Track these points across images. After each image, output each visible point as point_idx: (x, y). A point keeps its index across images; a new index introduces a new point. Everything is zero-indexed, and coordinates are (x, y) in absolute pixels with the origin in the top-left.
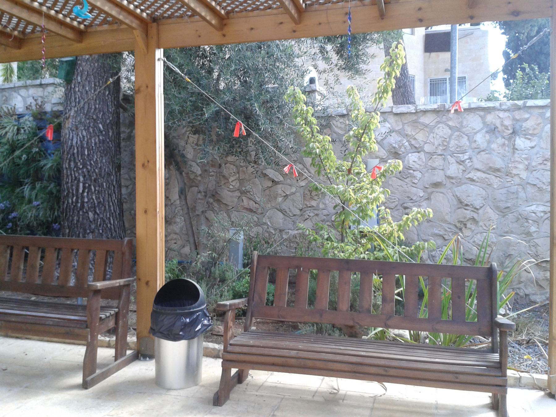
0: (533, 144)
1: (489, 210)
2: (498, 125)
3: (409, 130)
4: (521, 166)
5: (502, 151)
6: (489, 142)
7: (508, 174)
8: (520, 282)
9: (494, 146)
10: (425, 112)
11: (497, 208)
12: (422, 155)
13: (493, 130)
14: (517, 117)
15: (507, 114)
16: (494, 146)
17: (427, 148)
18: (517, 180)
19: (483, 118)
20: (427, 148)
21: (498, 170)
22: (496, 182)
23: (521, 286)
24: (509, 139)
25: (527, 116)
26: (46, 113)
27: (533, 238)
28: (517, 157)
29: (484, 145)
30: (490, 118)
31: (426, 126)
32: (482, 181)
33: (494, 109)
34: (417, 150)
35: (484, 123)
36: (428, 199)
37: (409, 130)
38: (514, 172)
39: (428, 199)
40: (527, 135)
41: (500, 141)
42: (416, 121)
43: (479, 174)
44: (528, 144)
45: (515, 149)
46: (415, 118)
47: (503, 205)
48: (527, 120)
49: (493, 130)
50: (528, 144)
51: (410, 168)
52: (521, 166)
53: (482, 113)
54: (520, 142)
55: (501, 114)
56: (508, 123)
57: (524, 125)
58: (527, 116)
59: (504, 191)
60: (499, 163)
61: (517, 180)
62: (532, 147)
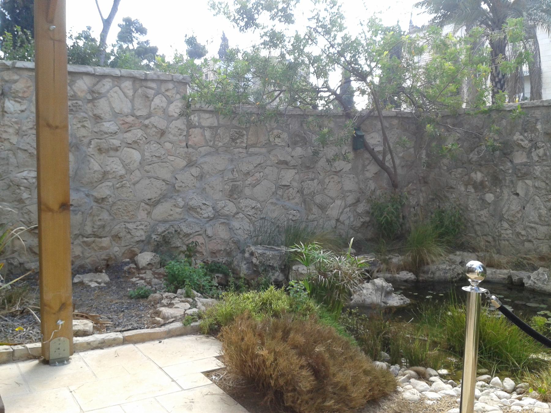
0: (23, 107)
4: (11, 130)
8: (14, 252)
14: (7, 78)
18: (7, 145)
23: (15, 255)
25: (16, 77)
27: (25, 205)
28: (6, 121)
48: (15, 82)
57: (14, 86)
58: (16, 77)
61: (7, 145)
62: (22, 111)
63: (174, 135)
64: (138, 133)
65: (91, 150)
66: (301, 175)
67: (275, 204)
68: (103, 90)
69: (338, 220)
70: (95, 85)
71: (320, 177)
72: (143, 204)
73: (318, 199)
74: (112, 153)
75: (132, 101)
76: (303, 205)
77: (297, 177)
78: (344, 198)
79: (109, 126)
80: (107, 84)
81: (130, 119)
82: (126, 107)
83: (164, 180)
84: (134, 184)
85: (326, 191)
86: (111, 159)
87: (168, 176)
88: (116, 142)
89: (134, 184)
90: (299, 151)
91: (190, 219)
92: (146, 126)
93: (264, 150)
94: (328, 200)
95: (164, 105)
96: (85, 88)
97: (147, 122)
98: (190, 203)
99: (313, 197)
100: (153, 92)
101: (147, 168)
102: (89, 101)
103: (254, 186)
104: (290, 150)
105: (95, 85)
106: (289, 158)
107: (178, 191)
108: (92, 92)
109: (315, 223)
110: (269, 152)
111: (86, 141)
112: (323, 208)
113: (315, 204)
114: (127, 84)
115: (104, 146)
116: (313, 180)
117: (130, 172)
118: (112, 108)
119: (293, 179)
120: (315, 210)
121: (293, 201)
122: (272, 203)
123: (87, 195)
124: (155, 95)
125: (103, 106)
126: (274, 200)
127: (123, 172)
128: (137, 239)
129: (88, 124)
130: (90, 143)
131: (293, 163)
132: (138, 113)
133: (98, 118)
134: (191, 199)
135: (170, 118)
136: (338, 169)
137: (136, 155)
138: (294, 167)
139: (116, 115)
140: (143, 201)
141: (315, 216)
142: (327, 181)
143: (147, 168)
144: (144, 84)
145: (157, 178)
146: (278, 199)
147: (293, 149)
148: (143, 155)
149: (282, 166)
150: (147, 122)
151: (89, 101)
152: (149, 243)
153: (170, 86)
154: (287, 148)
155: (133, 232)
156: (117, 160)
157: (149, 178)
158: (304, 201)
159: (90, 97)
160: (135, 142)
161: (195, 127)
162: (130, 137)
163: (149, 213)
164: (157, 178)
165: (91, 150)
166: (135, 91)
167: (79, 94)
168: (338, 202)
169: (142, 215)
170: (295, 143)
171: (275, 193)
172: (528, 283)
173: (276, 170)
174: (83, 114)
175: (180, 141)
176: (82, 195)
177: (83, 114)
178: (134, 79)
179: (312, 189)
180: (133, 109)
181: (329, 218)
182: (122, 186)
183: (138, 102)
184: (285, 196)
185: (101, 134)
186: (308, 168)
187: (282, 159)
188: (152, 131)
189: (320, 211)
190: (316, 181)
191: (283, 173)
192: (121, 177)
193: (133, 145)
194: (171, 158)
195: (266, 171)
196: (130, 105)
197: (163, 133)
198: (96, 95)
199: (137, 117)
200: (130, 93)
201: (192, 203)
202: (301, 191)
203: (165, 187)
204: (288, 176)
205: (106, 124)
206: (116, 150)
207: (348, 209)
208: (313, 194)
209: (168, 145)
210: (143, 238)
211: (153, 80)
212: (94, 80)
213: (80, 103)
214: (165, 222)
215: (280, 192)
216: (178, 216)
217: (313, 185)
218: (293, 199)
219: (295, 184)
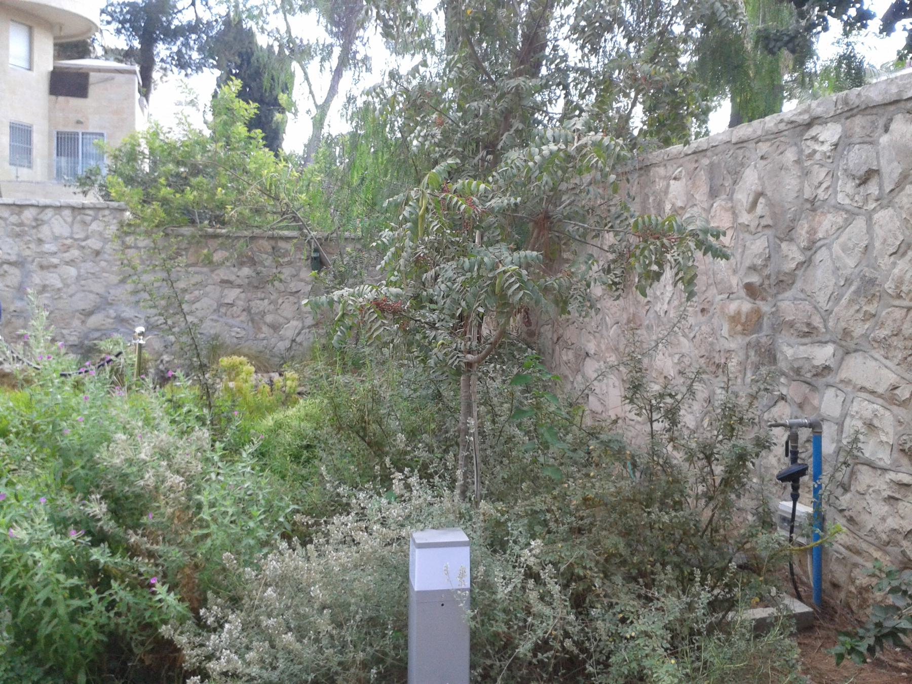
63: (110, 255)
64: (75, 253)
65: (34, 267)
66: (249, 294)
67: (216, 321)
68: (46, 218)
69: (293, 341)
70: (38, 214)
71: (272, 297)
72: (77, 314)
73: (269, 318)
74: (52, 270)
75: (71, 226)
76: (250, 324)
77: (243, 296)
78: (301, 319)
79: (49, 247)
80: (49, 213)
81: (69, 241)
82: (65, 231)
83: (98, 294)
84: (71, 296)
85: (279, 311)
86: (51, 275)
87: (101, 291)
88: (55, 261)
89: (71, 296)
90: (246, 271)
91: (122, 330)
92: (83, 247)
93: (205, 270)
94: (281, 320)
95: (101, 229)
96: (30, 216)
97: (83, 244)
98: (123, 315)
99: (263, 317)
100: (90, 218)
101: (83, 282)
103: (194, 303)
104: (235, 270)
105: (38, 214)
106: (232, 278)
107: (111, 304)
108: (36, 220)
109: (265, 342)
110: (212, 271)
111: (30, 259)
112: (275, 327)
113: (265, 323)
114: (67, 213)
115: (45, 263)
116: (263, 299)
117: (67, 286)
118: (53, 232)
119: (237, 298)
120: (265, 329)
121: (238, 319)
122: (212, 320)
124: (92, 221)
125: (45, 232)
126: (215, 317)
127: (60, 285)
128: (70, 343)
129: (32, 246)
130: (33, 261)
131: (239, 281)
132: (76, 236)
133: (40, 241)
134: (124, 311)
135: (106, 241)
136: (294, 290)
137: (72, 271)
138: (239, 286)
139: (56, 238)
140: (77, 311)
141: (263, 335)
142: (280, 301)
143: (83, 282)
144: (83, 211)
145: (91, 292)
146: (219, 316)
147: (240, 269)
148: (79, 272)
149: (226, 285)
150: (83, 244)
151: (34, 227)
152: (82, 347)
153: (107, 212)
154: (232, 269)
155: (67, 337)
156: (54, 275)
157: (84, 291)
158: (252, 320)
159: (34, 224)
160: (72, 261)
161: (129, 247)
162: (67, 256)
163: (83, 322)
164: (91, 292)
165: (34, 267)
166: (74, 218)
167: (26, 222)
168: (294, 323)
169: (76, 323)
170: (242, 264)
171: (217, 311)
172: (723, 475)
173: (218, 289)
174: (28, 238)
175: (115, 260)
177: (28, 238)
178: (73, 208)
179: (261, 309)
180: (72, 233)
181: (282, 339)
182: (60, 298)
183: (77, 227)
184: (229, 313)
185: (43, 254)
186: (257, 287)
187: (226, 278)
188: (88, 251)
189: (272, 331)
190: (266, 301)
191: (226, 291)
192: (59, 289)
193: (71, 263)
194: (105, 275)
195: (208, 289)
196: (69, 230)
197: (97, 253)
198: (39, 222)
199: (76, 240)
200: (69, 220)
201: (123, 315)
202: (247, 310)
203: (98, 300)
204: (232, 294)
205: (47, 246)
206: (55, 266)
207: (307, 330)
208: (263, 314)
209: (103, 264)
210: (76, 343)
211: (89, 208)
213: (26, 229)
214: (97, 330)
215: (223, 310)
216: (108, 326)
217: (259, 305)
218: (238, 317)
219: (240, 303)
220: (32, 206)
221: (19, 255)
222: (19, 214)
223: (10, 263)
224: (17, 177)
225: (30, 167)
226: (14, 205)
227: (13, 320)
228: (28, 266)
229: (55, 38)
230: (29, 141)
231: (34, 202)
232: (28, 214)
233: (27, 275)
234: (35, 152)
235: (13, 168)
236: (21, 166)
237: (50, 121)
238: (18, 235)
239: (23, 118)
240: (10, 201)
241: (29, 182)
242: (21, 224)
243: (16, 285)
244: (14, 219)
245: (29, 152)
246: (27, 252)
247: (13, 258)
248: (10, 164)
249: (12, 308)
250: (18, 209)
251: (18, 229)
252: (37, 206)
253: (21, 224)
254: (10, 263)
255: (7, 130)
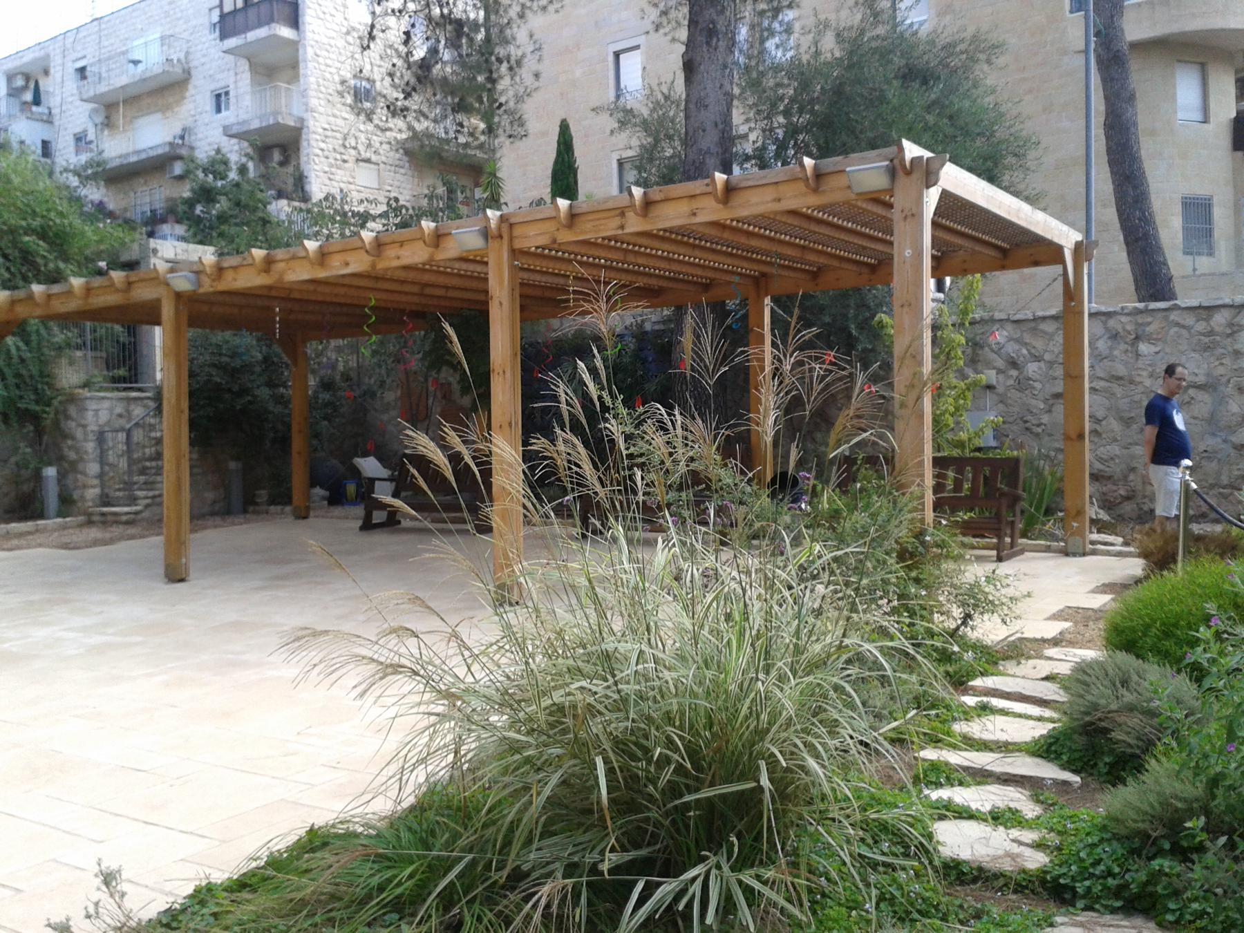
0: (1157, 349)
1: (1112, 420)
2: (1120, 330)
3: (1028, 338)
4: (1145, 373)
5: (1124, 358)
6: (1111, 348)
7: (1132, 382)
9: (1116, 353)
10: (1044, 318)
11: (1121, 419)
12: (1042, 364)
13: (1115, 336)
14: (1140, 321)
15: (1129, 318)
16: (1116, 353)
17: (1047, 357)
18: (1140, 389)
19: (1105, 323)
20: (1047, 357)
21: (1121, 378)
22: (1119, 391)
24: (1133, 345)
25: (1149, 319)
26: (646, 333)
28: (1140, 364)
29: (1106, 353)
30: (1112, 323)
31: (1045, 333)
32: (1105, 390)
33: (1115, 313)
34: (1037, 359)
35: (1107, 329)
36: (1050, 411)
37: (1028, 338)
38: (1138, 379)
39: (1050, 411)
40: (1150, 339)
41: (1123, 347)
42: (1035, 329)
43: (1102, 384)
44: (1153, 349)
45: (1138, 355)
46: (1033, 324)
47: (1126, 415)
48: (1149, 323)
49: (1115, 336)
50: (1153, 349)
51: (1030, 379)
52: (1145, 373)
53: (1103, 318)
54: (1143, 348)
55: (1124, 319)
56: (1128, 327)
58: (1149, 319)
59: (1126, 400)
60: (1121, 370)
61: (1140, 389)
62: (1157, 353)
65: (1230, 390)
70: (1235, 317)
96: (1223, 321)
102: (1229, 335)
108: (1231, 325)
111: (1224, 380)
123: (1225, 441)
130: (1229, 381)
151: (1229, 335)
159: (1229, 331)
165: (1230, 390)
167: (1217, 329)
174: (1222, 351)
176: (1219, 440)
177: (1222, 351)
198: (1235, 328)
212: (1233, 311)
213: (1218, 338)
220: (1224, 306)
221: (1208, 375)
222: (1207, 320)
223: (1199, 387)
224: (1195, 270)
225: (1211, 254)
226: (1200, 307)
227: (1204, 463)
228: (1222, 388)
229: (1237, 72)
230: (1208, 218)
231: (1227, 301)
232: (1220, 319)
233: (1222, 401)
234: (1217, 233)
235: (1190, 258)
236: (1199, 254)
237: (1235, 187)
238: (1207, 348)
239: (1199, 189)
240: (1195, 303)
241: (1213, 274)
242: (1211, 333)
243: (1206, 415)
244: (1201, 326)
245: (1209, 233)
246: (1221, 370)
247: (1201, 379)
248: (1186, 253)
249: (1202, 447)
250: (1204, 314)
251: (1206, 340)
252: (1232, 306)
253: (1211, 333)
254: (1199, 387)
255: (1178, 208)
